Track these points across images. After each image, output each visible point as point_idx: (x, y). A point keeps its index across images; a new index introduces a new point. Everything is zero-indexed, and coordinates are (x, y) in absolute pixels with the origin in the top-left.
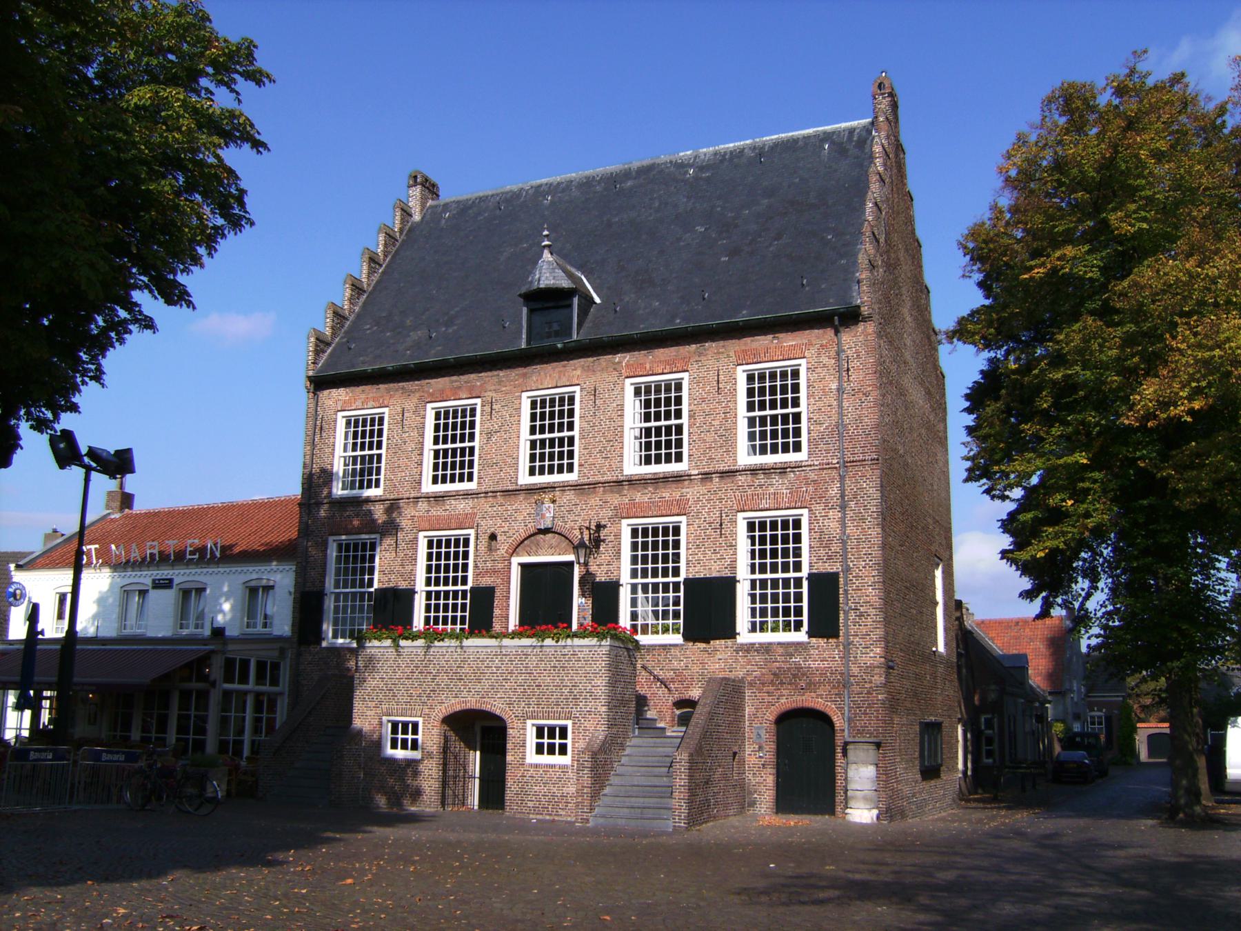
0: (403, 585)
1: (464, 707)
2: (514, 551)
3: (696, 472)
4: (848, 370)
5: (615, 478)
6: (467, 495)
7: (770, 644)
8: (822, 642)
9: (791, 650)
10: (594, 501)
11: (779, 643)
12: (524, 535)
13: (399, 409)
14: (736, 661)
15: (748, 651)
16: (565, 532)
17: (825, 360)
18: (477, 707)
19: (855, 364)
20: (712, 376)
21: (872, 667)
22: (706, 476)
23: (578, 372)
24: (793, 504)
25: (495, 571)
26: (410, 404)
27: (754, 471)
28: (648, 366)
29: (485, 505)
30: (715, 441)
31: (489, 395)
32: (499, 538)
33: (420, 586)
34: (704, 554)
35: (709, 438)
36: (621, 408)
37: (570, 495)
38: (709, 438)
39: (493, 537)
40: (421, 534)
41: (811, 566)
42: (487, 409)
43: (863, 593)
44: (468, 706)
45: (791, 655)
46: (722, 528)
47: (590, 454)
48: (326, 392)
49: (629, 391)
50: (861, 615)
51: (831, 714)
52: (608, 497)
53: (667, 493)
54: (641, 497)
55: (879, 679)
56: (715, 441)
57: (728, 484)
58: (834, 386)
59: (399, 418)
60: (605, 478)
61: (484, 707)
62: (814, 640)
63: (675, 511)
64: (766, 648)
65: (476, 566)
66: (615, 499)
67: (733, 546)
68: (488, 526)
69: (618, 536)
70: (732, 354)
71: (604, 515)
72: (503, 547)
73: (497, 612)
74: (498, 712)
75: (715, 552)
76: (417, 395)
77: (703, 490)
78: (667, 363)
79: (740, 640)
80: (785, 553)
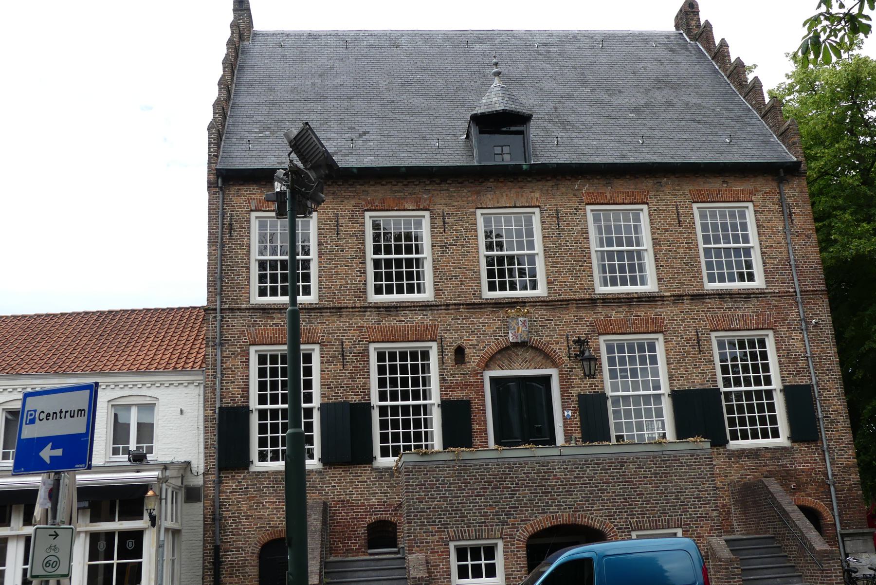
0: (354, 399)
1: (555, 522)
2: (487, 366)
3: (669, 294)
4: (790, 215)
5: (587, 297)
6: (425, 306)
7: (758, 449)
8: (804, 447)
9: (778, 454)
10: (569, 316)
11: (766, 449)
12: (495, 349)
13: (331, 214)
14: (731, 467)
15: (739, 457)
16: (540, 346)
17: (770, 205)
18: (572, 520)
19: (795, 210)
20: (671, 209)
21: (847, 466)
22: (678, 298)
23: (537, 195)
24: (760, 326)
25: (465, 385)
26: (345, 209)
27: (721, 295)
28: (608, 196)
29: (447, 318)
30: (682, 267)
31: (439, 209)
32: (467, 351)
33: (254, 404)
34: (686, 369)
35: (676, 263)
36: (585, 231)
37: (539, 313)
38: (676, 263)
39: (460, 352)
40: (372, 347)
41: (783, 379)
42: (439, 222)
43: (832, 403)
44: (560, 521)
45: (779, 459)
46: (699, 344)
47: (559, 272)
48: (233, 189)
49: (590, 217)
50: (832, 422)
51: (821, 510)
52: (582, 313)
53: (643, 312)
54: (616, 314)
55: (855, 477)
56: (682, 267)
57: (698, 307)
58: (780, 227)
59: (333, 223)
60: (577, 297)
61: (579, 521)
62: (796, 445)
63: (652, 329)
64: (755, 453)
65: (443, 380)
66: (590, 316)
67: (711, 361)
68: (453, 339)
69: (597, 350)
70: (687, 192)
71: (582, 330)
72: (473, 361)
73: (475, 426)
74: (597, 525)
75: (695, 367)
76: (353, 202)
77: (676, 310)
78: (627, 194)
79: (729, 447)
80: (756, 369)
